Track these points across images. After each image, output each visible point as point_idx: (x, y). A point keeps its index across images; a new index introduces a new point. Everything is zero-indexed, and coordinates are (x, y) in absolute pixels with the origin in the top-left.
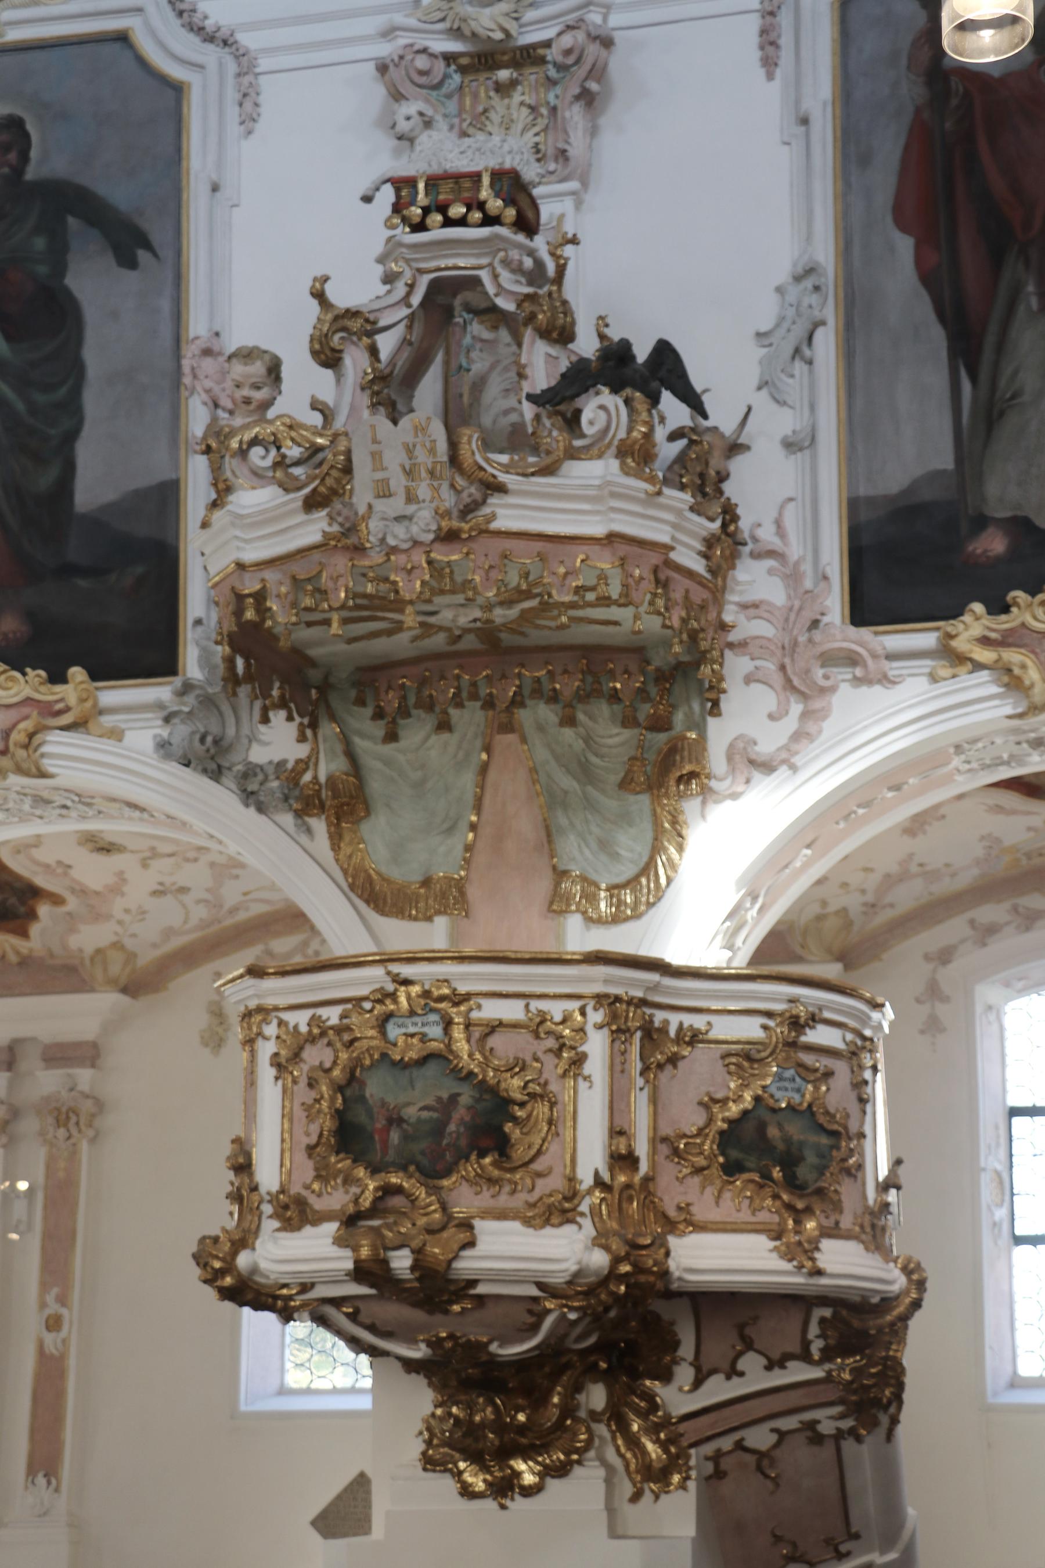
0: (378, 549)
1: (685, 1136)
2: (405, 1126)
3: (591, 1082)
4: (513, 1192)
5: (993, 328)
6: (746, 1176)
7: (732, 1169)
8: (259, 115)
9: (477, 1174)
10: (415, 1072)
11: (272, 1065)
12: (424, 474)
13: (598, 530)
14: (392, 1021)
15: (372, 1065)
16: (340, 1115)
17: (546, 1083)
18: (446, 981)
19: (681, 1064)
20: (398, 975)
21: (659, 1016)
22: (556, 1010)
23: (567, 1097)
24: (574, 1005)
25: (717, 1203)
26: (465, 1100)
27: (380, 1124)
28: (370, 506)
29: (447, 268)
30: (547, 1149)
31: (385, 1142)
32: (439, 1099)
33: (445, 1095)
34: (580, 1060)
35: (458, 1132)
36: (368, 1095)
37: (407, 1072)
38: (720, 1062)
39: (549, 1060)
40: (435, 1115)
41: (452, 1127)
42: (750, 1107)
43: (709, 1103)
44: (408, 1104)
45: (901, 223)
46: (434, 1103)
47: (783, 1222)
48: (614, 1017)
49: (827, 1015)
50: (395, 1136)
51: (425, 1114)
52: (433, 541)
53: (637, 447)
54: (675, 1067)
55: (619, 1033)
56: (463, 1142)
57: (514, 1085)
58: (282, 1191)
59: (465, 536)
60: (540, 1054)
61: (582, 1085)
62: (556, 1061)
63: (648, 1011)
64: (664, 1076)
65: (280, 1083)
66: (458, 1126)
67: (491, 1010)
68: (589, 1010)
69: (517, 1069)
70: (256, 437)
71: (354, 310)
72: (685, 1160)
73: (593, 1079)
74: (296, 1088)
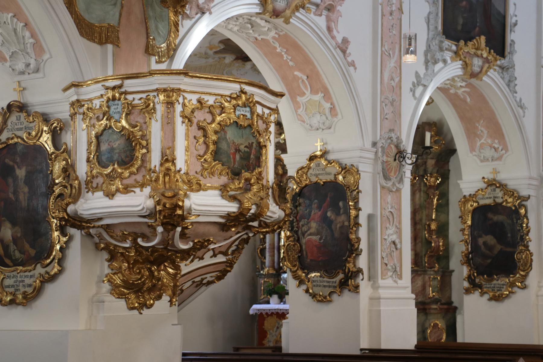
11: (181, 116)
26: (254, 145)
31: (234, 159)
33: (251, 143)
36: (228, 138)
41: (252, 156)
44: (242, 144)
51: (246, 149)
65: (184, 125)
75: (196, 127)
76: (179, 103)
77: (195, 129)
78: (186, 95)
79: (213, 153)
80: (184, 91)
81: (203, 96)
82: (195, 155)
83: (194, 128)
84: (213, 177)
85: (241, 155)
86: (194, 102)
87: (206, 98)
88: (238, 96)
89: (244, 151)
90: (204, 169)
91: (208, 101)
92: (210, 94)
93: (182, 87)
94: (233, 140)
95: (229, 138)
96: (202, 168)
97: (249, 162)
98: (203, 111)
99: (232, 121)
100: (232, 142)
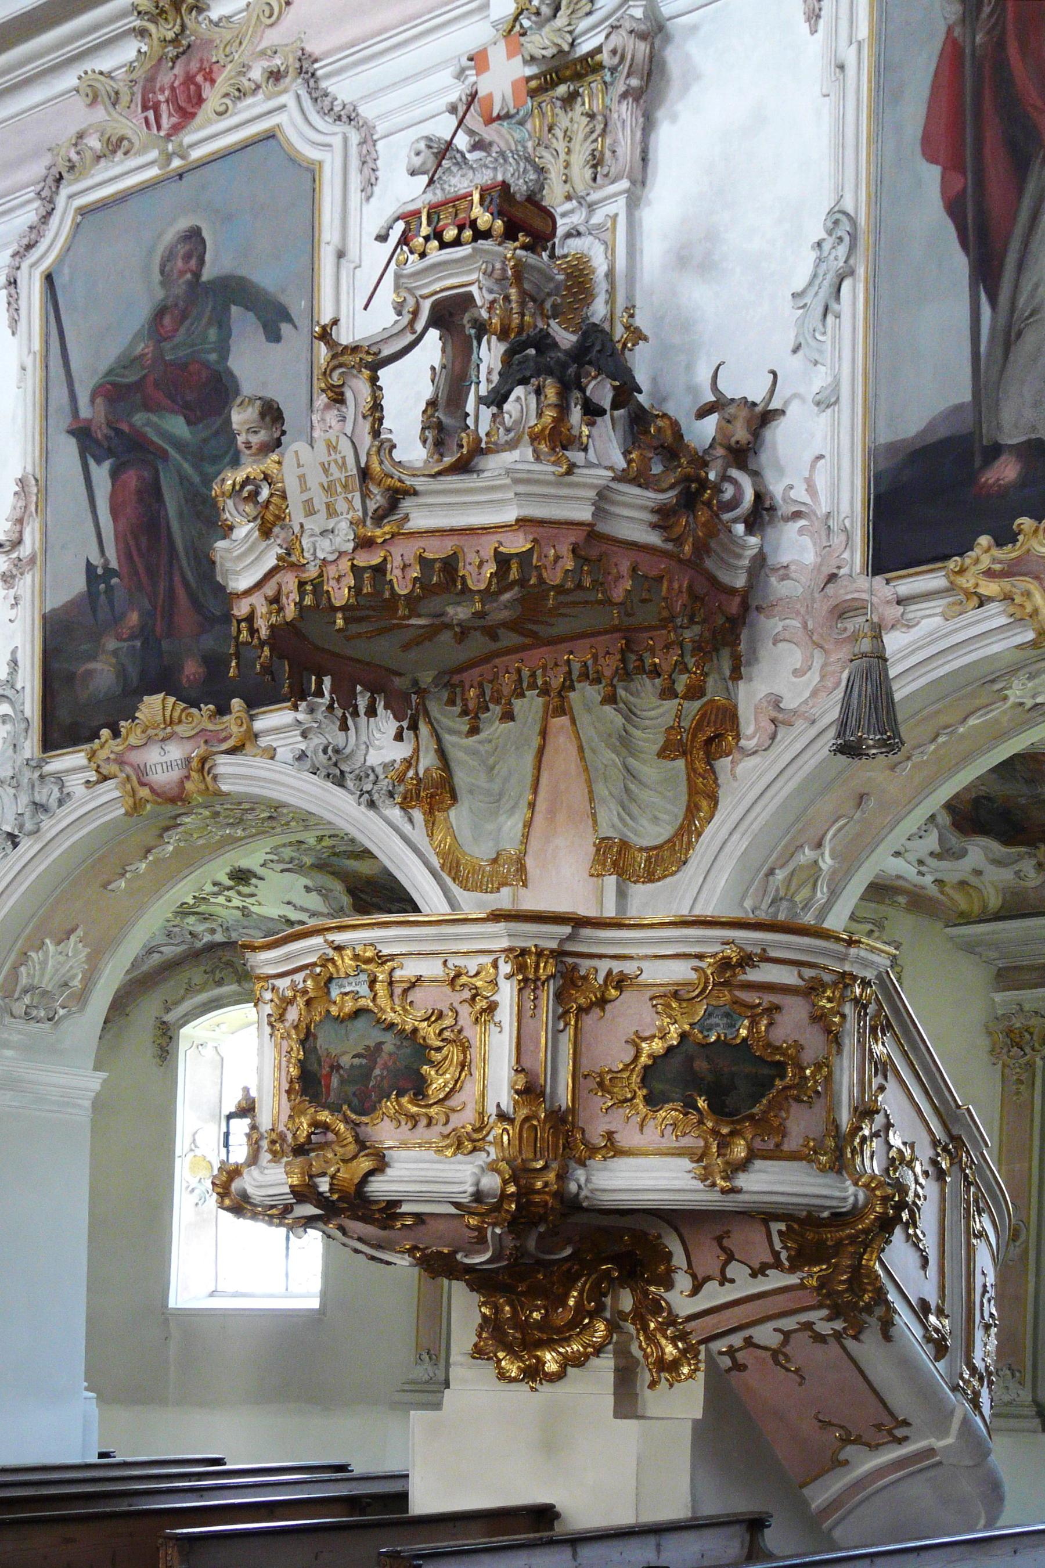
0: (313, 563)
1: (610, 1071)
2: (342, 1072)
4: (429, 1125)
5: (1015, 245)
6: (671, 1105)
7: (653, 1101)
8: (377, 179)
9: (397, 1112)
10: (349, 1024)
12: (339, 490)
13: (510, 515)
14: (334, 982)
15: (321, 1021)
16: (302, 1064)
17: (460, 1031)
18: (371, 945)
19: (608, 1007)
20: (333, 942)
21: (585, 965)
22: (472, 965)
23: (476, 1042)
24: (487, 960)
25: (641, 1130)
26: (388, 1048)
27: (326, 1070)
28: (302, 526)
29: (442, 290)
30: (461, 1088)
33: (372, 1044)
34: (492, 1008)
35: (383, 1078)
38: (649, 1003)
39: (465, 1010)
40: (364, 1061)
41: (377, 1072)
42: (675, 1043)
43: (636, 1042)
44: (344, 1053)
45: (930, 154)
47: (707, 1147)
48: (521, 968)
49: (773, 954)
50: (335, 1081)
51: (356, 1061)
52: (354, 550)
53: (547, 432)
54: (603, 1010)
55: (528, 983)
56: (385, 1084)
57: (429, 1032)
58: (273, 1130)
59: (380, 540)
60: (455, 1005)
62: (471, 1009)
63: (570, 960)
64: (589, 1021)
67: (409, 970)
68: (501, 962)
69: (433, 1019)
70: (248, 478)
71: (354, 345)
72: (609, 1093)
85: (341, 1076)
89: (352, 1065)
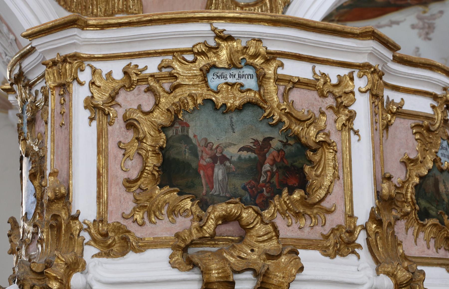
3: (358, 135)
11: (86, 107)
26: (275, 144)
27: (205, 160)
32: (256, 142)
33: (260, 139)
34: (351, 117)
35: (271, 171)
37: (228, 117)
40: (253, 155)
41: (267, 167)
44: (230, 145)
46: (251, 145)
51: (245, 154)
56: (275, 180)
61: (354, 138)
62: (335, 117)
65: (94, 123)
66: (271, 165)
73: (360, 133)
74: (110, 128)
75: (123, 125)
76: (81, 84)
77: (120, 128)
78: (97, 65)
79: (155, 173)
80: (92, 58)
81: (135, 62)
82: (121, 180)
83: (118, 127)
84: (158, 221)
86: (118, 75)
87: (141, 63)
88: (210, 48)
89: (240, 158)
90: (140, 207)
91: (146, 68)
92: (148, 54)
93: (85, 51)
94: (206, 140)
95: (195, 136)
96: (134, 205)
97: (259, 182)
98: (135, 91)
99: (199, 101)
100: (203, 143)
